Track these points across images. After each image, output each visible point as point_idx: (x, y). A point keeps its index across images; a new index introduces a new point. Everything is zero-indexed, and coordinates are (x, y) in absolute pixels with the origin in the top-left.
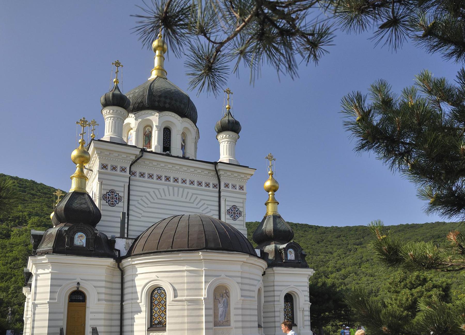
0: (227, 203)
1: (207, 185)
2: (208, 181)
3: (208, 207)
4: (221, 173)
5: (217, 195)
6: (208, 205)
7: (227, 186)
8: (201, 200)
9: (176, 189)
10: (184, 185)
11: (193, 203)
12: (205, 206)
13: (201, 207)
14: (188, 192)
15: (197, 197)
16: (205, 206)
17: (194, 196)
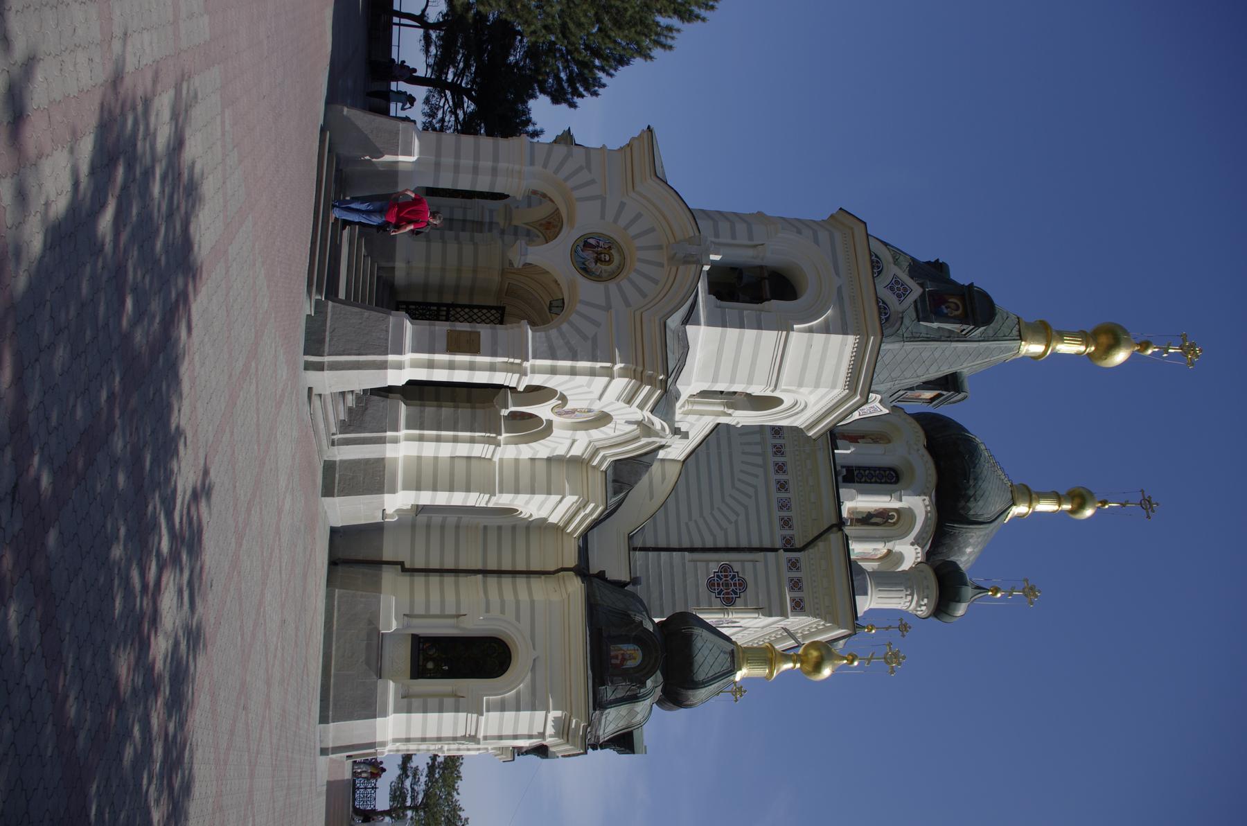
0: (749, 566)
1: (786, 523)
2: (795, 522)
3: (730, 522)
4: (821, 544)
5: (767, 544)
6: (736, 522)
7: (794, 565)
8: (746, 508)
9: (758, 449)
10: (771, 468)
11: (733, 486)
12: (733, 518)
13: (727, 505)
14: (757, 476)
15: (750, 497)
16: (733, 518)
17: (751, 491)
